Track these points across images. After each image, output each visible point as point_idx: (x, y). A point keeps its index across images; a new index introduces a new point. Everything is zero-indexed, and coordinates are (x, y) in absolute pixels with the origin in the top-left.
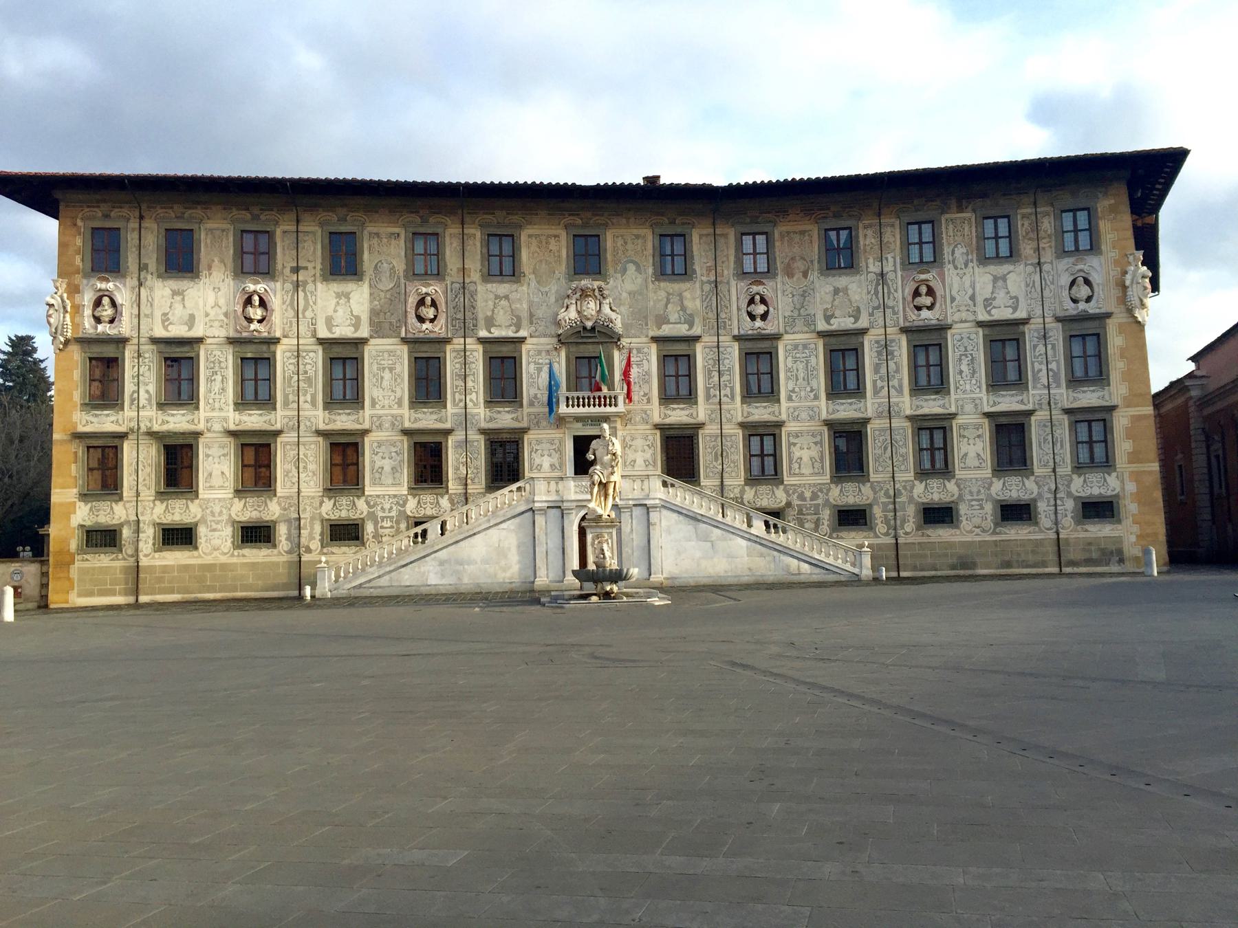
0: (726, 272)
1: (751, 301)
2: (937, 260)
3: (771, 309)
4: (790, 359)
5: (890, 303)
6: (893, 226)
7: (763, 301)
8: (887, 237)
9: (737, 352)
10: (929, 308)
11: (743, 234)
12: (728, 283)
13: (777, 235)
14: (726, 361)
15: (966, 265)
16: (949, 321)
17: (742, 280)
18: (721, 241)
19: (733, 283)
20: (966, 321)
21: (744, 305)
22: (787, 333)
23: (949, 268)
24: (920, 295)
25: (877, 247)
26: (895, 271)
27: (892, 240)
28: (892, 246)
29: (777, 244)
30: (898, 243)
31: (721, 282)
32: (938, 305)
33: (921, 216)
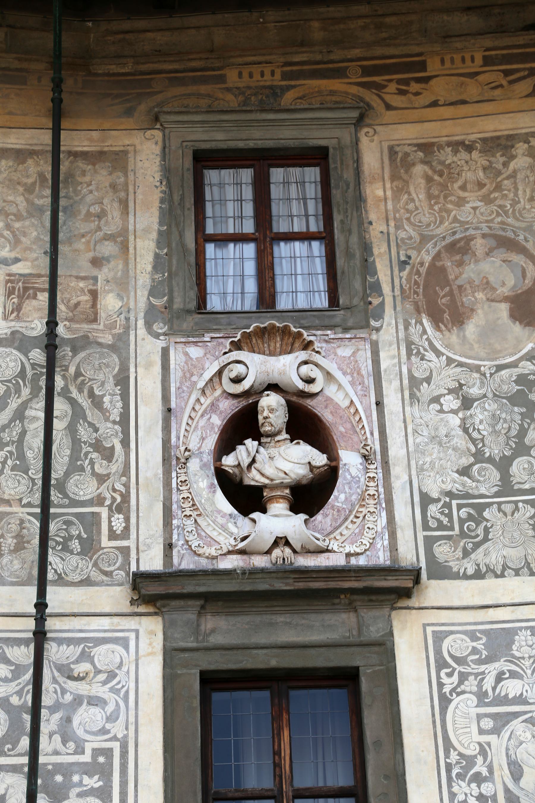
0: (110, 303)
1: (243, 426)
3: (350, 460)
4: (464, 707)
7: (305, 425)
9: (152, 672)
11: (206, 159)
12: (120, 346)
13: (372, 156)
14: (86, 718)
17: (194, 335)
18: (92, 187)
19: (147, 347)
21: (202, 436)
22: (440, 572)
29: (376, 191)
31: (79, 345)
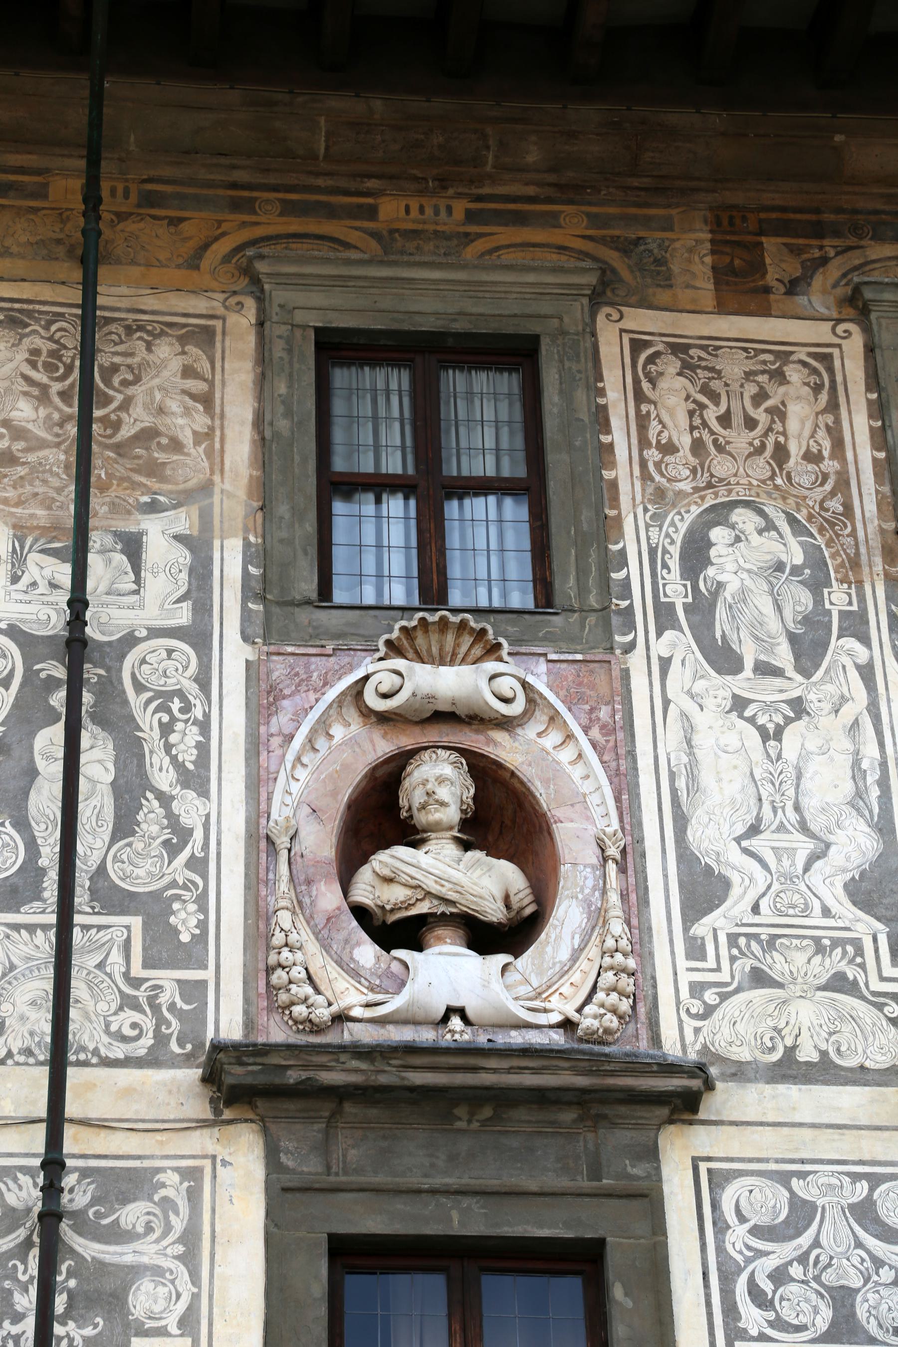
2: (568, 590)
5: (140, 867)
6: (204, 336)
8: (156, 390)
10: (502, 936)
15: (809, 648)
16: (677, 1039)
20: (825, 1071)
23: (663, 673)
24: (411, 835)
25: (59, 459)
26: (198, 636)
27: (185, 423)
28: (192, 465)
30: (239, 447)
32: (567, 919)
33: (430, 295)
